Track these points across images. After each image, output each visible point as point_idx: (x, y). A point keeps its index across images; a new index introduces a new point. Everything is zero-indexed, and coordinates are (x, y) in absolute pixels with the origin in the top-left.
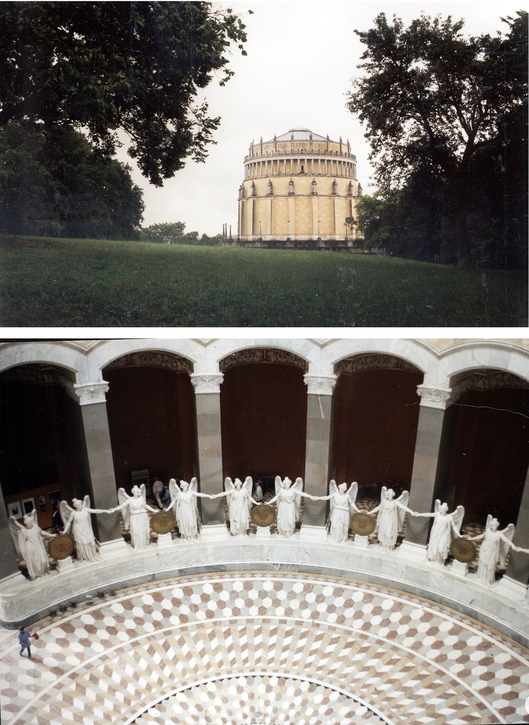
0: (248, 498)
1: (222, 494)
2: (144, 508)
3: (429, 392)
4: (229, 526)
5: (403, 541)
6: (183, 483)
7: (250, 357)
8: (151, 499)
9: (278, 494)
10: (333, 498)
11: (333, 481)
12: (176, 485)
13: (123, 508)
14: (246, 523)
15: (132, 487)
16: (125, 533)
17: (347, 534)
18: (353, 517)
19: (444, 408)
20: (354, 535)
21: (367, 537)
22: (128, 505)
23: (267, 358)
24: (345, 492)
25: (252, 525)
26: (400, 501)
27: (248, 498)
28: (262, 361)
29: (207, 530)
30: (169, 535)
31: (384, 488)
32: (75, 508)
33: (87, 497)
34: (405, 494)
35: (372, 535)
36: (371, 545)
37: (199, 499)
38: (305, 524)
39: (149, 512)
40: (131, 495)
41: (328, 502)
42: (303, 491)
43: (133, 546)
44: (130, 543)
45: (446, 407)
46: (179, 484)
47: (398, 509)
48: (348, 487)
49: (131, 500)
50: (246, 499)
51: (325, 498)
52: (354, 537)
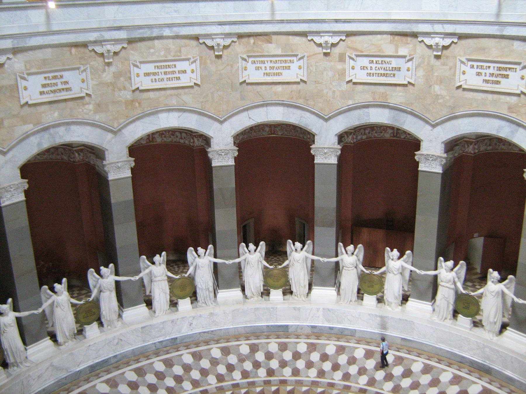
0: (261, 262)
1: (237, 260)
2: (164, 275)
3: (427, 157)
4: (243, 290)
5: (409, 299)
6: (201, 250)
7: (259, 131)
8: (170, 265)
9: (290, 258)
10: (342, 260)
11: (341, 244)
12: (194, 253)
13: (145, 274)
15: (155, 255)
16: (147, 298)
17: (356, 294)
18: (362, 277)
19: (441, 172)
20: (363, 294)
21: (376, 296)
22: (151, 272)
23: (274, 132)
24: (353, 254)
25: (266, 288)
26: (404, 261)
27: (261, 262)
28: (270, 134)
29: (223, 294)
30: (188, 300)
31: (388, 249)
32: (101, 276)
33: (111, 265)
34: (408, 254)
35: (380, 294)
36: (380, 305)
37: (215, 264)
38: (315, 286)
39: (169, 277)
40: (153, 263)
41: (337, 263)
42: (313, 254)
43: (155, 312)
44: (152, 308)
45: (442, 171)
46: (196, 251)
47: (403, 268)
48: (355, 248)
49: (152, 267)
50: (260, 263)
51: (334, 260)
52: (363, 297)
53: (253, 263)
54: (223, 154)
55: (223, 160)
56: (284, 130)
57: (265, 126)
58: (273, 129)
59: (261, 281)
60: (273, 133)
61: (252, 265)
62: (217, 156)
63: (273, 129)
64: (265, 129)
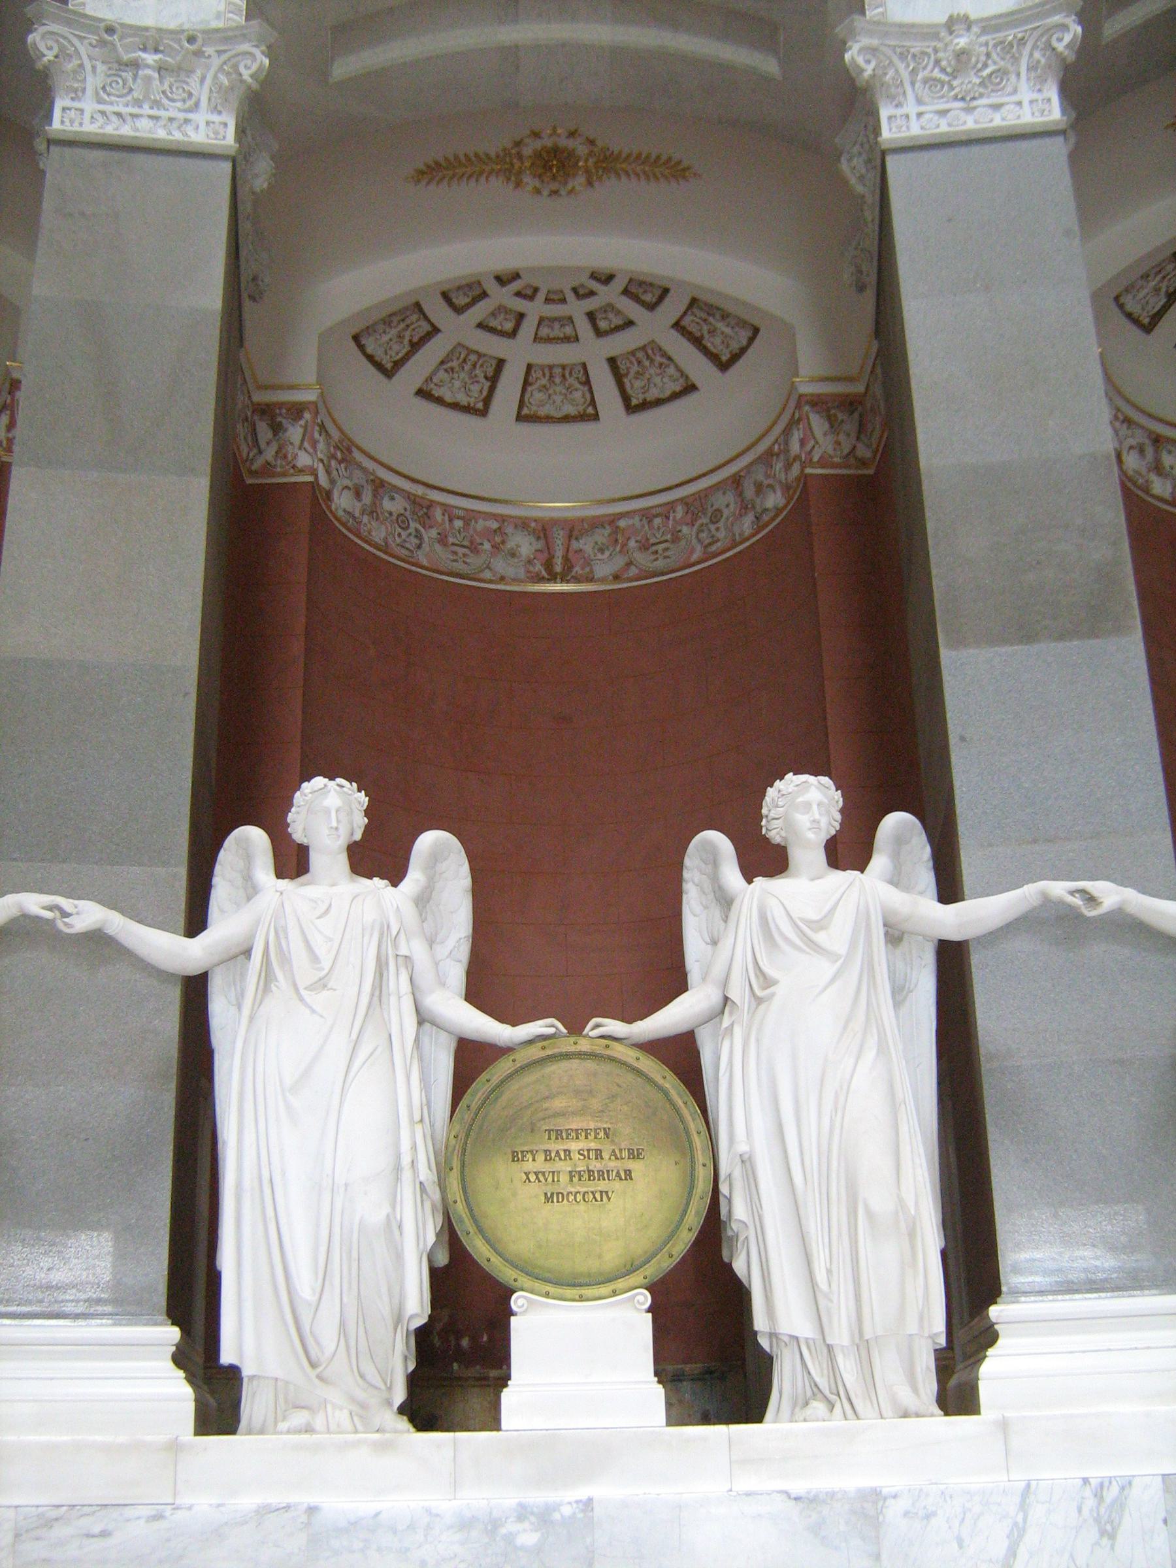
7: (474, 548)
14: (393, 1226)
23: (568, 565)
28: (540, 579)
50: (399, 983)
53: (321, 949)
54: (150, 58)
55: (146, 110)
56: (632, 543)
57: (509, 530)
58: (559, 553)
59: (408, 1192)
60: (558, 568)
61: (315, 958)
62: (101, 68)
63: (559, 553)
64: (510, 545)
